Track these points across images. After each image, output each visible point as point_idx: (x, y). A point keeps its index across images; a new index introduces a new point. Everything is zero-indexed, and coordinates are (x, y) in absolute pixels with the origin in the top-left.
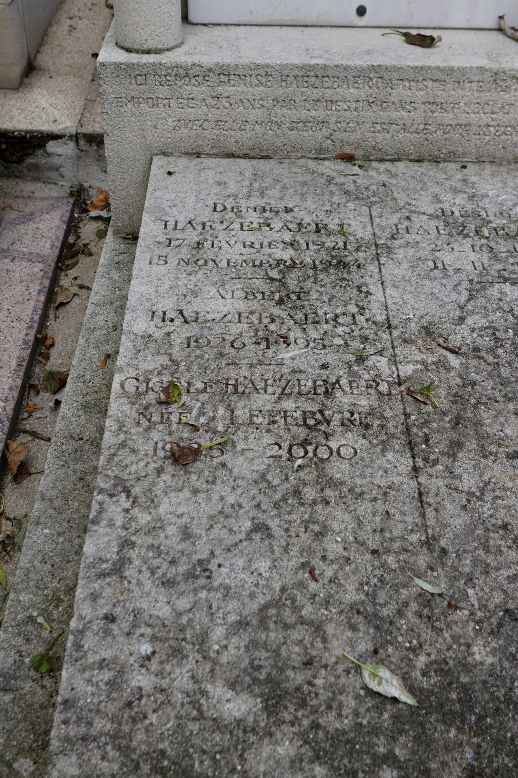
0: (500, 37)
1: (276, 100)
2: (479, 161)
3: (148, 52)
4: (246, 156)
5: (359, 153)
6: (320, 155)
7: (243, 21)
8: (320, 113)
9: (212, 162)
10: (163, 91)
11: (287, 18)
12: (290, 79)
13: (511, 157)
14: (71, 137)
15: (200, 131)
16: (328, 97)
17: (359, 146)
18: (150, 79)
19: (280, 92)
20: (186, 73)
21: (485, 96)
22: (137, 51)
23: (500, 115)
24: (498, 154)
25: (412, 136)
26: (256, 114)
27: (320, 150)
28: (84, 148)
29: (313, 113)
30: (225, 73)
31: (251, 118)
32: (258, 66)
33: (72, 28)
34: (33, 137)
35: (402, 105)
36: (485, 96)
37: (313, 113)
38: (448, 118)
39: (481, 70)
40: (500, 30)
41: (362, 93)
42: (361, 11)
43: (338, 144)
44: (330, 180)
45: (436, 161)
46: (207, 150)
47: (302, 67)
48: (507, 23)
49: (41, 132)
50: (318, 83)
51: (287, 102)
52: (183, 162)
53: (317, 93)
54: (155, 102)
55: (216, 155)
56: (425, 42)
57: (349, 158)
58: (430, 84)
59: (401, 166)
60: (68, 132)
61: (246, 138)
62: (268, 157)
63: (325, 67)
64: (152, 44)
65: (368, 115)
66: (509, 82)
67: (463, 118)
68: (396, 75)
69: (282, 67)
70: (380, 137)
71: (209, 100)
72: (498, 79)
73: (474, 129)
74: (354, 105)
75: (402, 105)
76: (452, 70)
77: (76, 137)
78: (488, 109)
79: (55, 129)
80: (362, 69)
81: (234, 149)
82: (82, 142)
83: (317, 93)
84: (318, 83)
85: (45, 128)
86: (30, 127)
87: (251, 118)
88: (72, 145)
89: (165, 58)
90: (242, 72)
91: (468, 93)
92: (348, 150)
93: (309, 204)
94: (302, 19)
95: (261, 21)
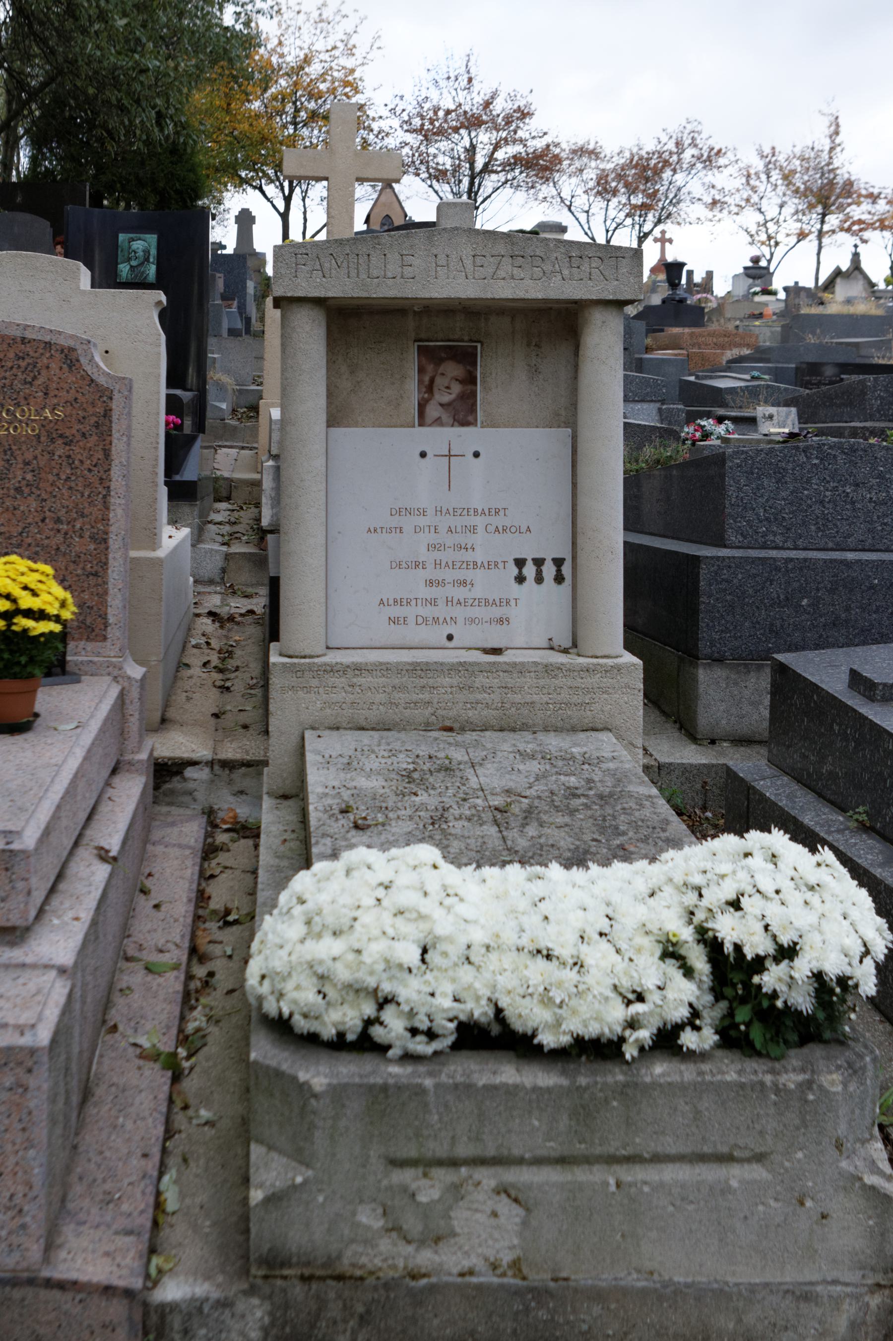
0: (551, 652)
1: (394, 687)
2: (546, 730)
3: (305, 657)
4: (373, 729)
5: (456, 726)
6: (427, 727)
7: (366, 645)
8: (426, 696)
9: (348, 732)
10: (315, 682)
11: (397, 643)
12: (404, 672)
13: (569, 727)
14: (207, 763)
15: (340, 711)
16: (430, 684)
17: (456, 720)
18: (306, 673)
19: (397, 681)
20: (331, 669)
21: (542, 682)
22: (297, 657)
23: (554, 696)
24: (559, 725)
25: (494, 712)
26: (380, 697)
27: (428, 724)
28: (218, 772)
29: (421, 696)
30: (358, 668)
31: (377, 701)
32: (381, 664)
33: (189, 699)
34: (174, 764)
35: (484, 689)
36: (542, 682)
37: (421, 696)
38: (518, 698)
39: (536, 664)
40: (552, 648)
41: (455, 681)
42: (450, 638)
43: (440, 719)
44: (436, 739)
45: (513, 730)
46: (344, 725)
47: (412, 664)
48: (555, 643)
49: (181, 759)
50: (423, 674)
51: (402, 688)
52: (327, 732)
53: (424, 681)
54: (308, 689)
55: (351, 729)
56: (497, 651)
57: (450, 729)
58: (501, 674)
59: (488, 733)
60: (204, 759)
61: (373, 715)
62: (389, 730)
63: (427, 663)
64: (307, 652)
65: (461, 697)
66: (556, 672)
67: (528, 699)
68: (476, 668)
69: (398, 663)
70: (470, 713)
71: (347, 688)
72: (549, 669)
73: (538, 706)
74: (449, 690)
75: (484, 689)
76: (515, 663)
77: (211, 764)
78: (545, 691)
79: (195, 756)
80: (453, 665)
81: (364, 724)
82: (216, 767)
83: (424, 681)
84: (423, 674)
85: (186, 755)
86: (172, 755)
87: (377, 701)
88: (207, 770)
89: (316, 660)
90: (370, 668)
91: (529, 680)
92: (448, 723)
93: (423, 748)
94: (408, 643)
95: (378, 645)
